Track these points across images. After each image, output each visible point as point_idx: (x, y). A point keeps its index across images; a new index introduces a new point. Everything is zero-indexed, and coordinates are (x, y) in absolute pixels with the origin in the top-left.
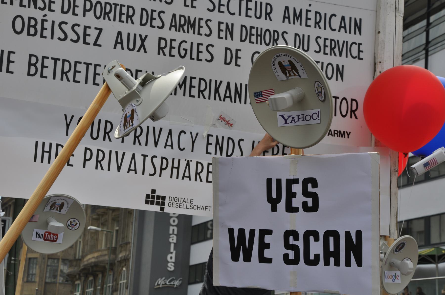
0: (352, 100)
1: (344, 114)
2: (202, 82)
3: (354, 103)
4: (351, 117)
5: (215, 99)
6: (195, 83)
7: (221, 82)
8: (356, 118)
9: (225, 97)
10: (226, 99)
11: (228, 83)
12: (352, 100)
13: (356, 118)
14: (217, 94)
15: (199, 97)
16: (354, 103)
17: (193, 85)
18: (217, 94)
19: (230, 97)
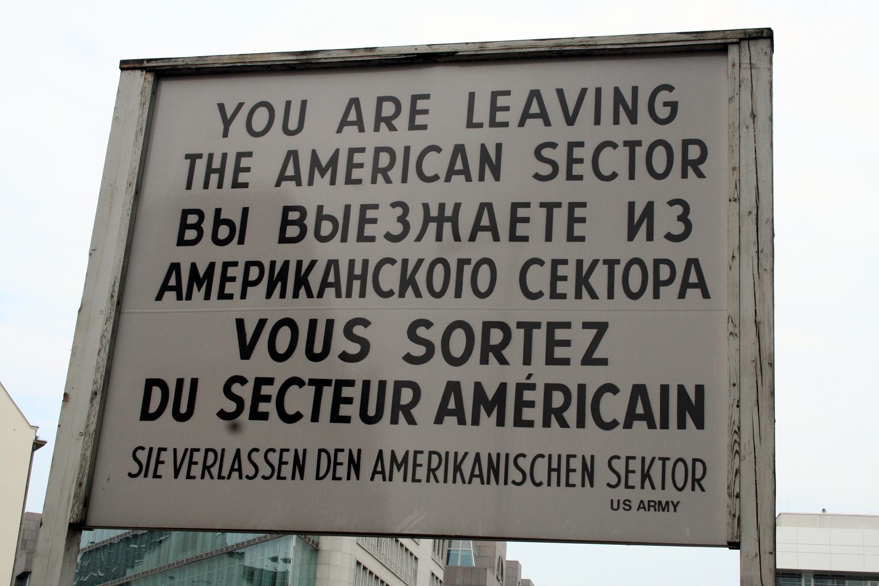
0: (695, 461)
1: (680, 485)
2: (435, 458)
3: (699, 465)
4: (693, 489)
5: (454, 481)
6: (422, 459)
7: (466, 454)
8: (703, 490)
9: (472, 475)
10: (474, 479)
11: (478, 455)
12: (695, 461)
13: (703, 490)
14: (458, 474)
15: (428, 481)
16: (699, 465)
17: (418, 462)
18: (458, 474)
19: (481, 476)
